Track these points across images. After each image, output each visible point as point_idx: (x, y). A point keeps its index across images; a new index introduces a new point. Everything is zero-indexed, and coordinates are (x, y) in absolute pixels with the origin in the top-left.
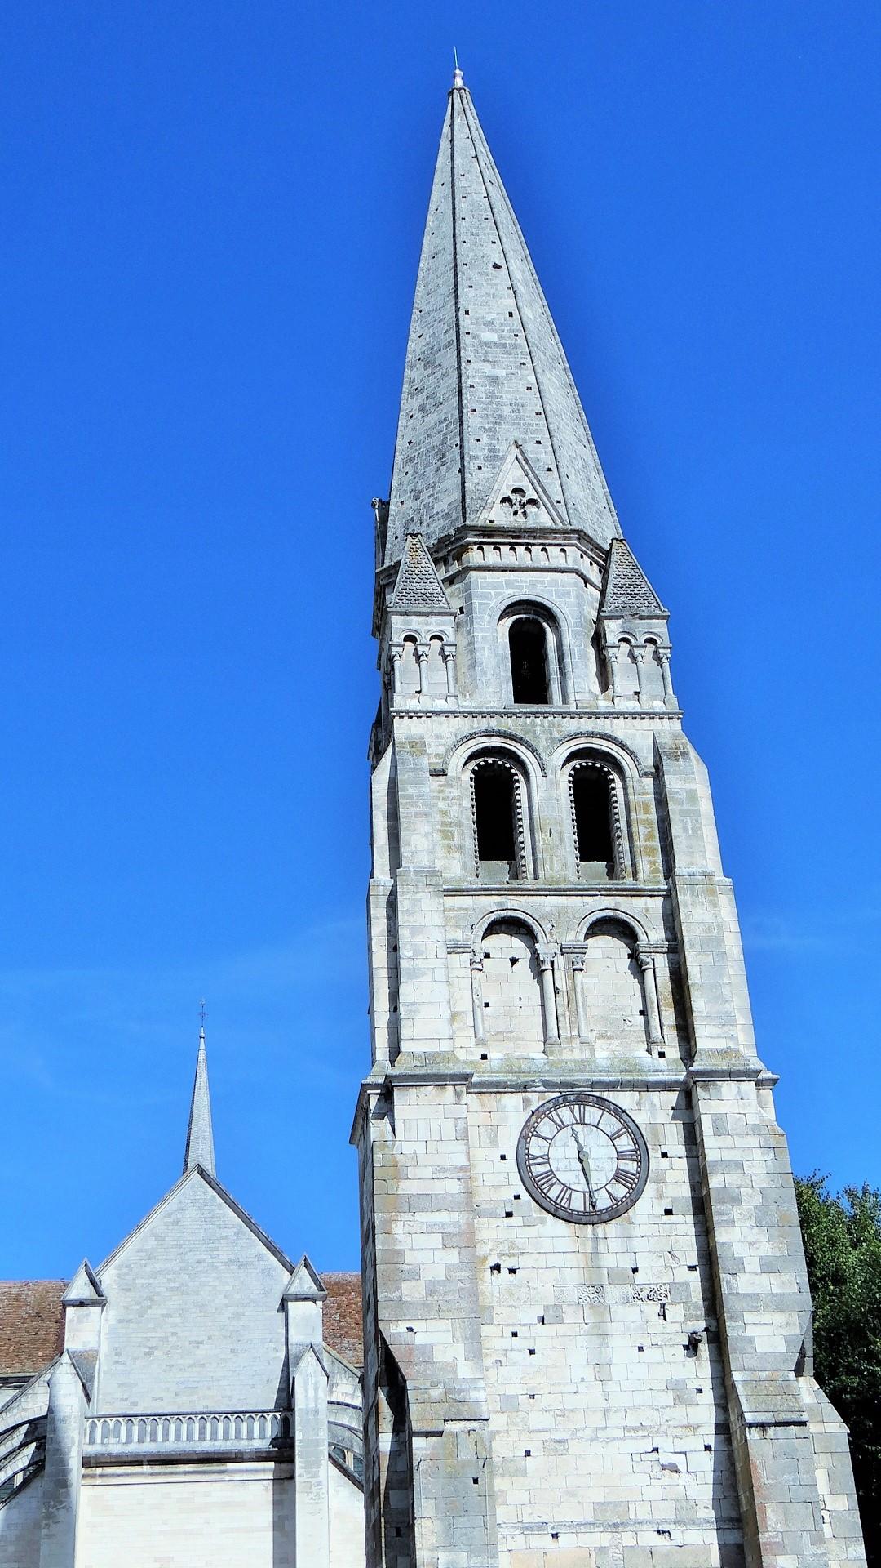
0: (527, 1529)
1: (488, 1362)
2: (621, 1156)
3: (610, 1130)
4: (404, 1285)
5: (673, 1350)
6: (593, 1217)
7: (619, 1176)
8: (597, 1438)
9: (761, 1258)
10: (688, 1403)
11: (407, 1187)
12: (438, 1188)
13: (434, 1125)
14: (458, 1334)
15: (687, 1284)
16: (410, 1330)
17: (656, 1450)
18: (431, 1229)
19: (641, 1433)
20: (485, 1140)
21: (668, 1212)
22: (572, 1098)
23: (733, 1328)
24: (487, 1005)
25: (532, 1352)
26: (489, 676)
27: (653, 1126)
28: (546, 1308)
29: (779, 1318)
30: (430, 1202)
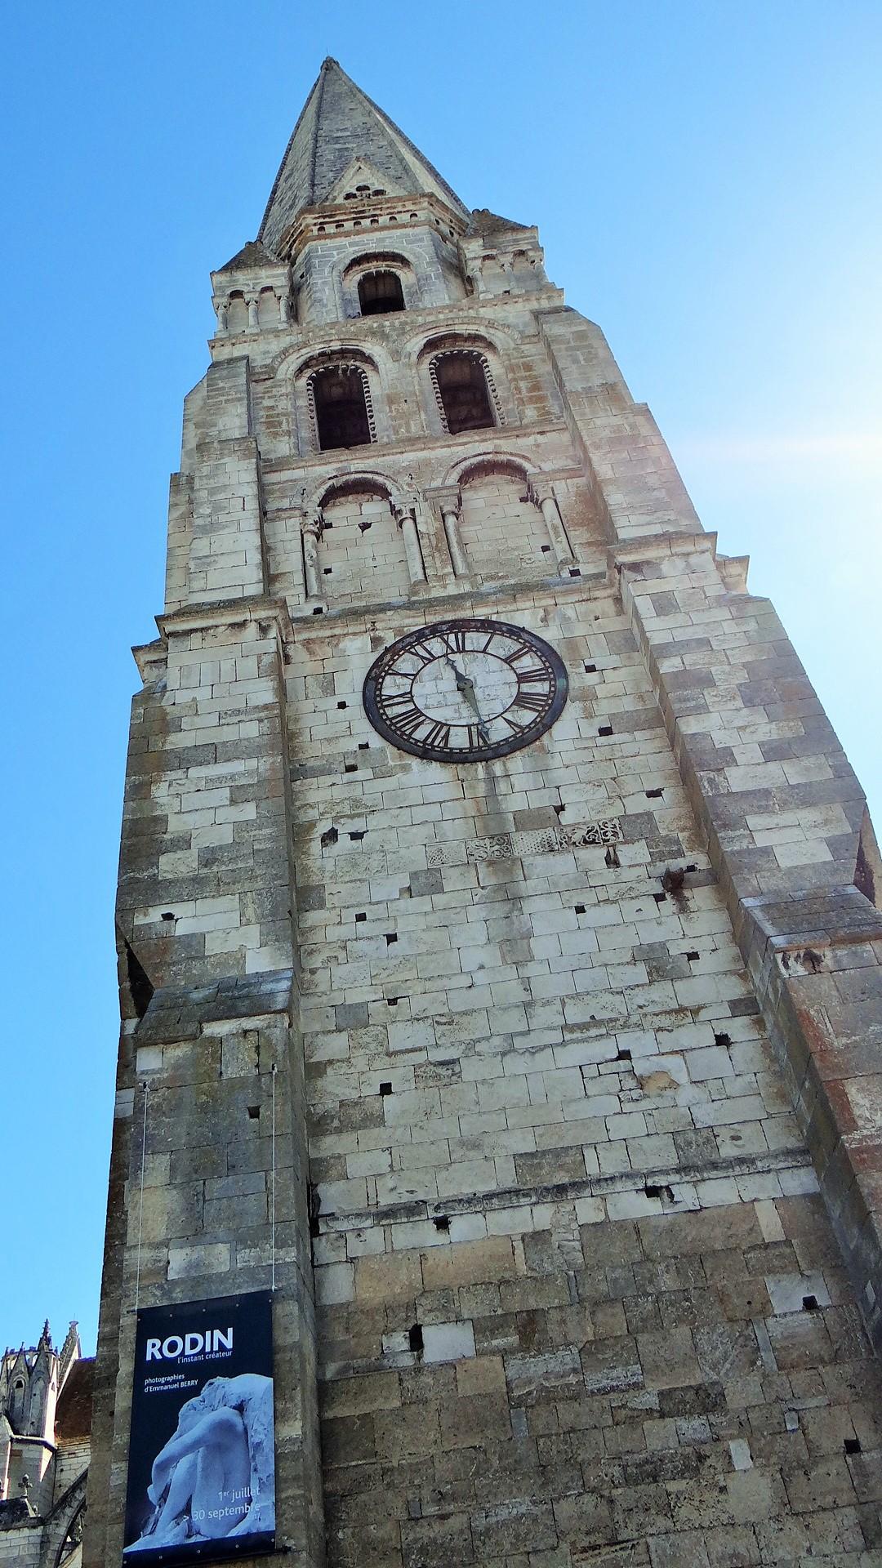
0: (387, 1215)
1: (316, 961)
2: (522, 678)
3: (502, 653)
4: (163, 859)
5: (637, 904)
6: (484, 752)
7: (521, 700)
8: (512, 1050)
9: (761, 744)
10: (675, 976)
11: (177, 741)
12: (228, 734)
13: (227, 666)
14: (250, 912)
15: (649, 815)
16: (168, 917)
17: (624, 1055)
18: (213, 783)
19: (593, 1032)
20: (314, 688)
21: (605, 732)
22: (444, 627)
23: (732, 840)
24: (328, 571)
25: (391, 938)
26: (330, 307)
27: (571, 643)
28: (414, 876)
29: (808, 816)
30: (213, 753)
